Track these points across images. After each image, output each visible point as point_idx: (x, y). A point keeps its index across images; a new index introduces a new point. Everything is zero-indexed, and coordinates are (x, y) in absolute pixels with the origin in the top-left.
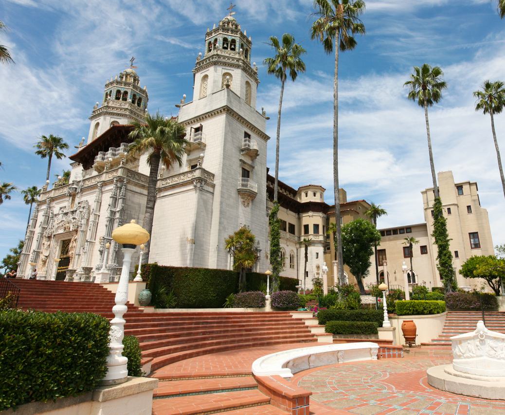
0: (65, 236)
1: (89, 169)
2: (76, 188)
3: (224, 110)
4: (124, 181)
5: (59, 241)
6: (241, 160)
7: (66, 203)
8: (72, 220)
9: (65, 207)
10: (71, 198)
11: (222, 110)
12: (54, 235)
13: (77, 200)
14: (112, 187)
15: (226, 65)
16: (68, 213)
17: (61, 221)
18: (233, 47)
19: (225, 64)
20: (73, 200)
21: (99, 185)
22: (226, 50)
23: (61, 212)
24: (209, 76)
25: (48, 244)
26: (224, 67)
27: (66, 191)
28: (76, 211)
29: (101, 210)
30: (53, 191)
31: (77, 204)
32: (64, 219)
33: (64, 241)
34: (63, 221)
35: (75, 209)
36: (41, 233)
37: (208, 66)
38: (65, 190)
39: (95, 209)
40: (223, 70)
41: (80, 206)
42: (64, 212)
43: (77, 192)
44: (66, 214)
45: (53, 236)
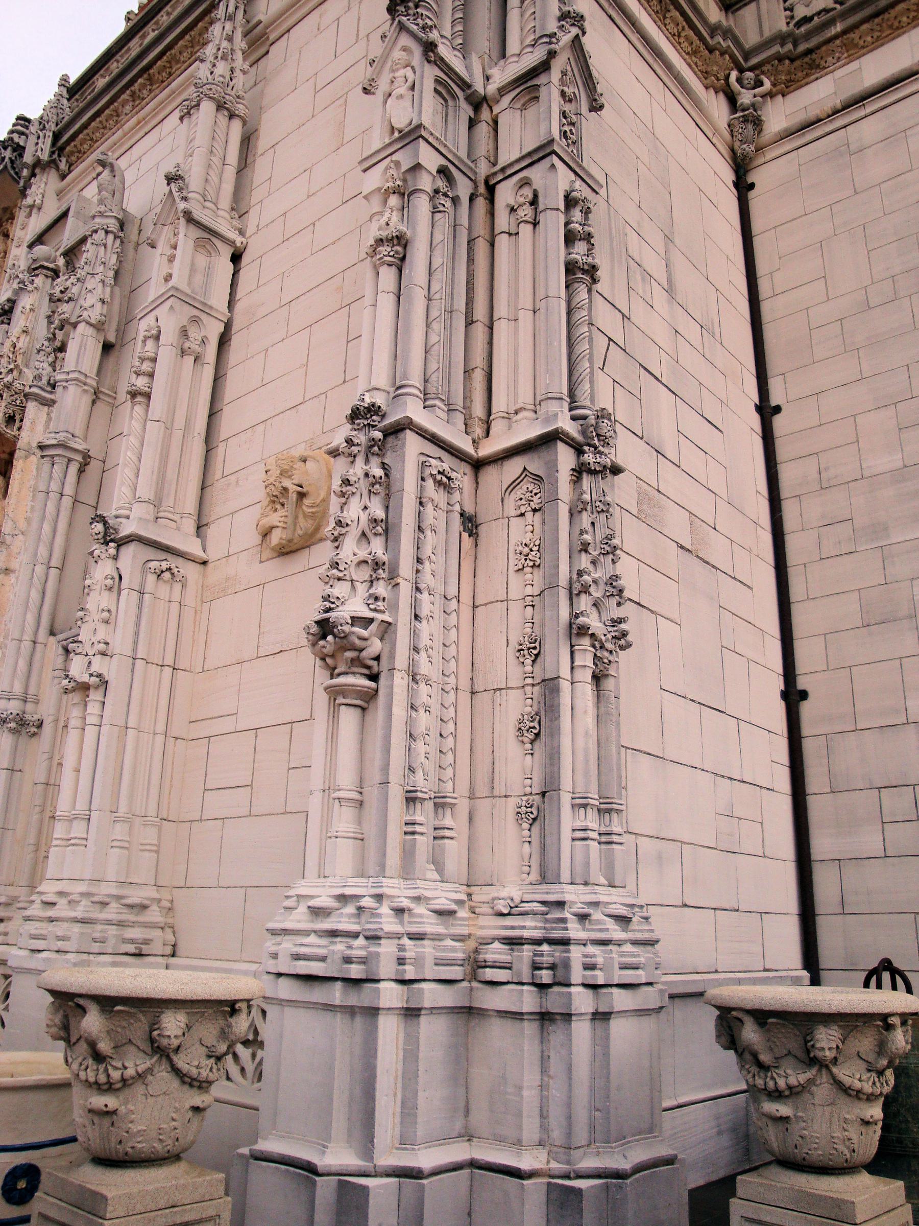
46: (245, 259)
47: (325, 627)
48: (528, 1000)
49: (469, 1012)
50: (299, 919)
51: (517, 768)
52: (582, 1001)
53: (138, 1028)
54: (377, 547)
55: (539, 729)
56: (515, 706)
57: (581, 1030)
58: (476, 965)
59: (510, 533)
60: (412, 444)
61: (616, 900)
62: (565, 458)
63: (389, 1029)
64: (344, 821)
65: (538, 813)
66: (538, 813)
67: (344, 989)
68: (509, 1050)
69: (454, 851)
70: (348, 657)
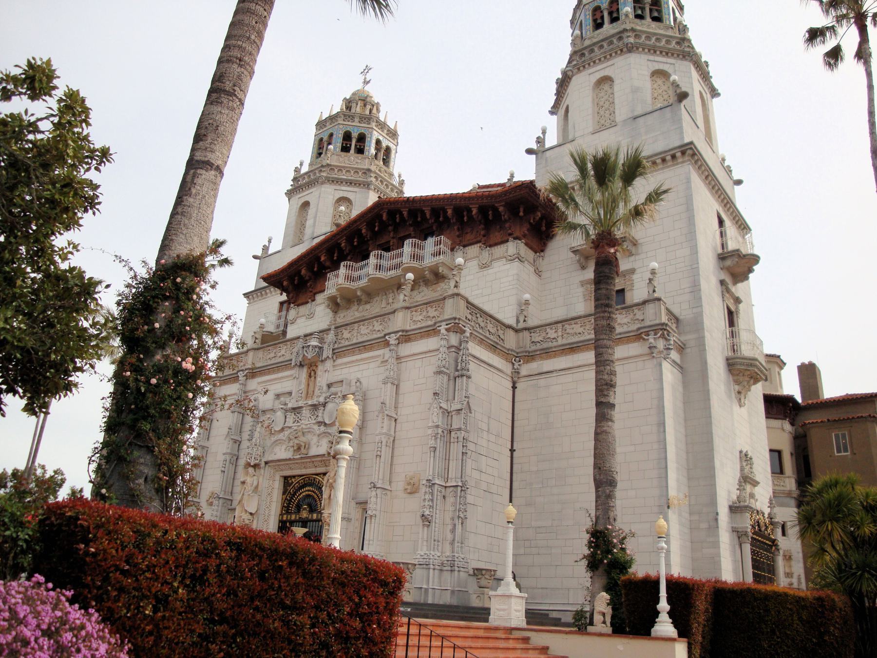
0: (292, 466)
1: (307, 303)
2: (320, 348)
3: (683, 153)
4: (464, 332)
5: (278, 478)
6: (722, 282)
7: (290, 382)
8: (316, 427)
9: (290, 393)
10: (304, 372)
11: (679, 154)
12: (266, 463)
13: (322, 379)
14: (431, 343)
15: (655, 52)
16: (301, 407)
17: (283, 430)
18: (656, 14)
19: (653, 50)
20: (312, 375)
21: (392, 340)
22: (643, 21)
23: (278, 405)
24: (617, 82)
25: (255, 483)
26: (652, 58)
27: (284, 353)
28: (324, 405)
29: (400, 405)
30: (251, 354)
31: (325, 388)
32: (290, 423)
33: (286, 478)
34: (290, 428)
35: (322, 400)
36: (230, 454)
37: (606, 58)
38: (283, 352)
39: (387, 403)
40: (649, 63)
41: (336, 394)
42: (290, 405)
43: (324, 356)
44: (296, 410)
45: (263, 464)
46: (398, 421)
47: (423, 515)
48: (449, 568)
49: (441, 570)
50: (418, 556)
51: (449, 536)
52: (456, 569)
53: (406, 566)
54: (430, 503)
55: (453, 531)
56: (450, 527)
57: (456, 573)
58: (442, 564)
59: (450, 500)
60: (436, 486)
61: (463, 556)
62: (459, 489)
63: (431, 571)
64: (425, 543)
65: (452, 543)
66: (452, 543)
67: (426, 566)
68: (447, 575)
69: (440, 548)
70: (426, 520)
